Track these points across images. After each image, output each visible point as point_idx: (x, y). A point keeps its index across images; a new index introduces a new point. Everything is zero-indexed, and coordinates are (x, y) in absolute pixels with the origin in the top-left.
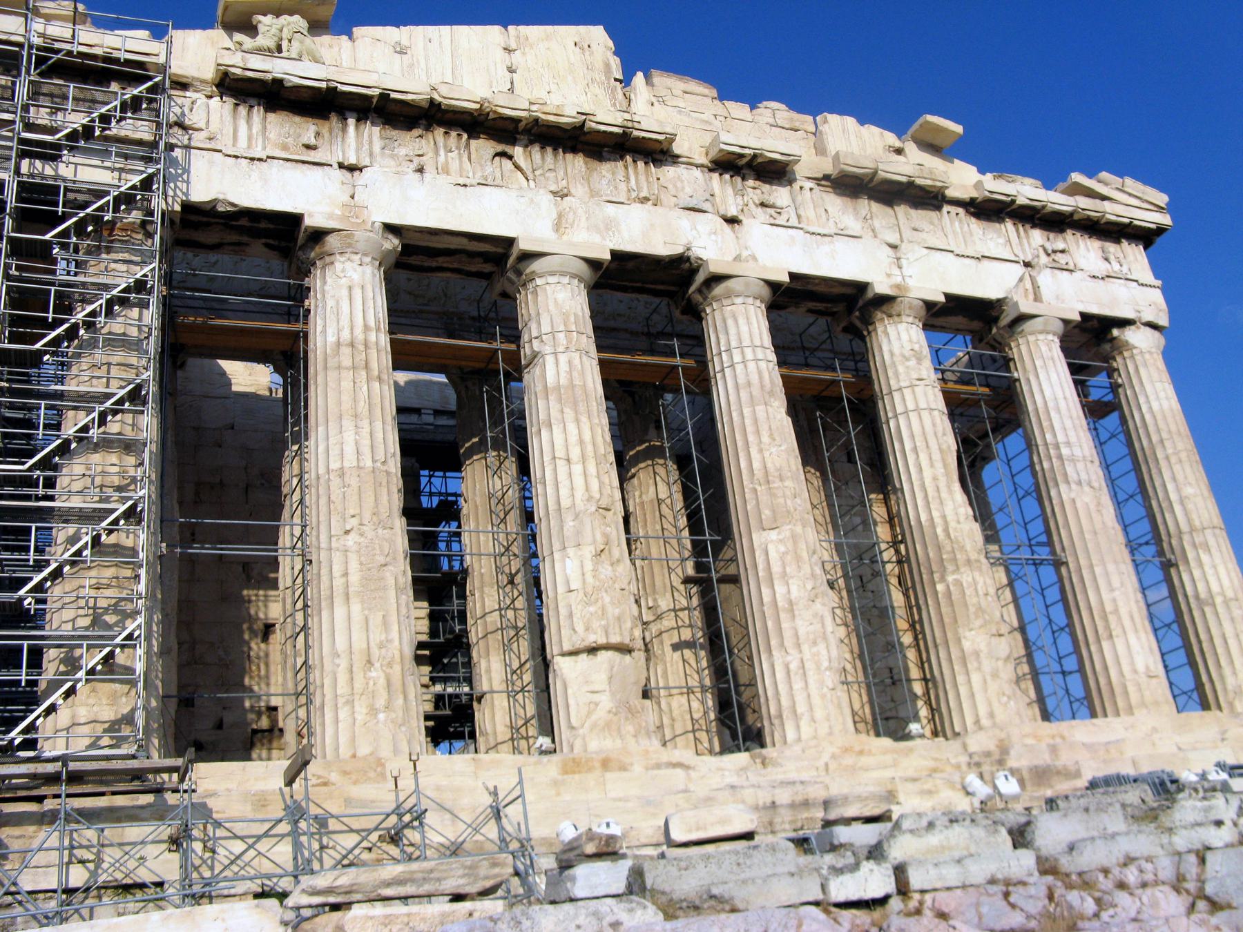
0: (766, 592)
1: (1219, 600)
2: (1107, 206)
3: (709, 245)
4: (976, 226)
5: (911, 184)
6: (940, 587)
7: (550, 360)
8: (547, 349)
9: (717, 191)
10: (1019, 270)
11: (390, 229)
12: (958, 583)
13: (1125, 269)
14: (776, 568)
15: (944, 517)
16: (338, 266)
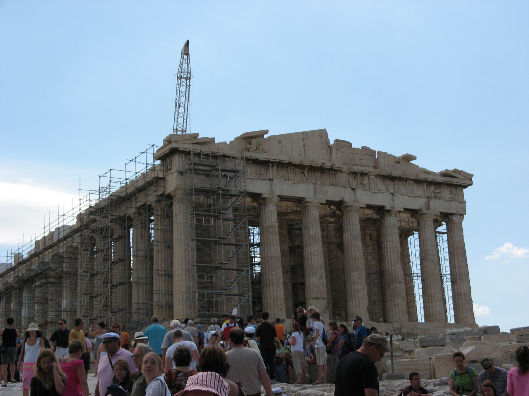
0: (353, 286)
1: (463, 294)
2: (454, 179)
3: (347, 196)
4: (415, 186)
5: (400, 177)
6: (392, 287)
7: (311, 229)
8: (311, 226)
9: (351, 181)
10: (425, 200)
11: (279, 196)
12: (396, 287)
13: (456, 198)
14: (356, 281)
15: (395, 270)
16: (268, 206)
